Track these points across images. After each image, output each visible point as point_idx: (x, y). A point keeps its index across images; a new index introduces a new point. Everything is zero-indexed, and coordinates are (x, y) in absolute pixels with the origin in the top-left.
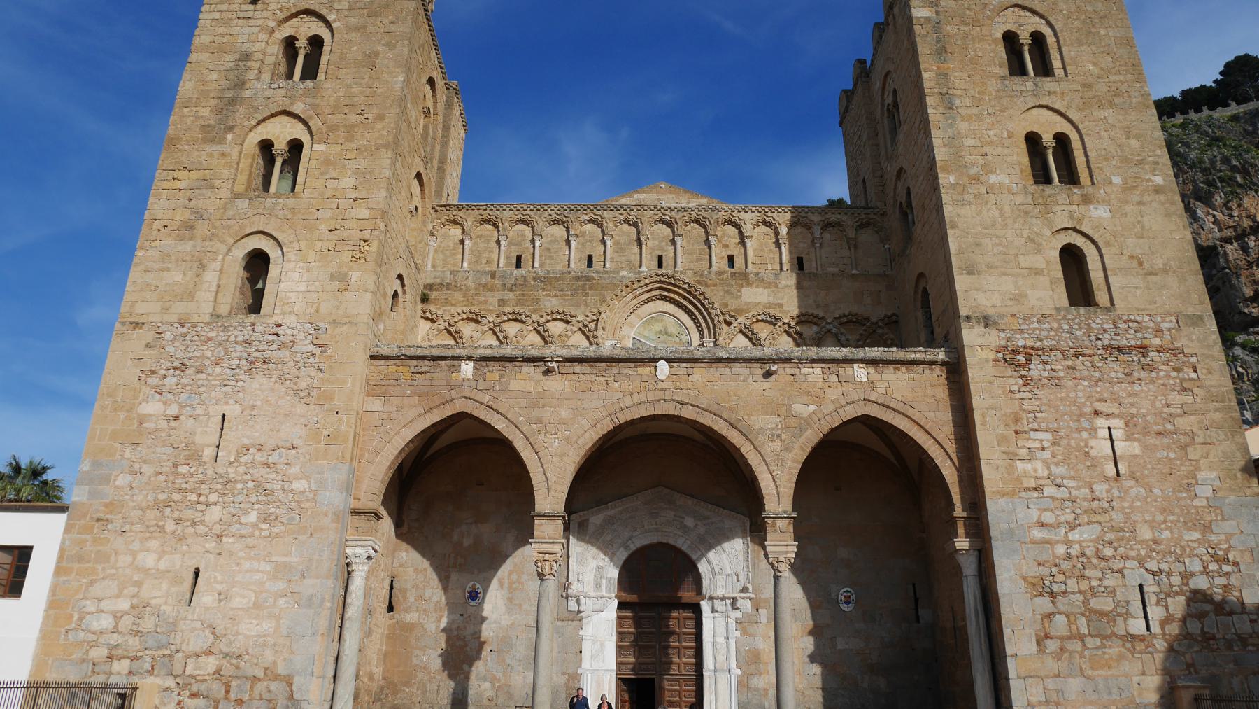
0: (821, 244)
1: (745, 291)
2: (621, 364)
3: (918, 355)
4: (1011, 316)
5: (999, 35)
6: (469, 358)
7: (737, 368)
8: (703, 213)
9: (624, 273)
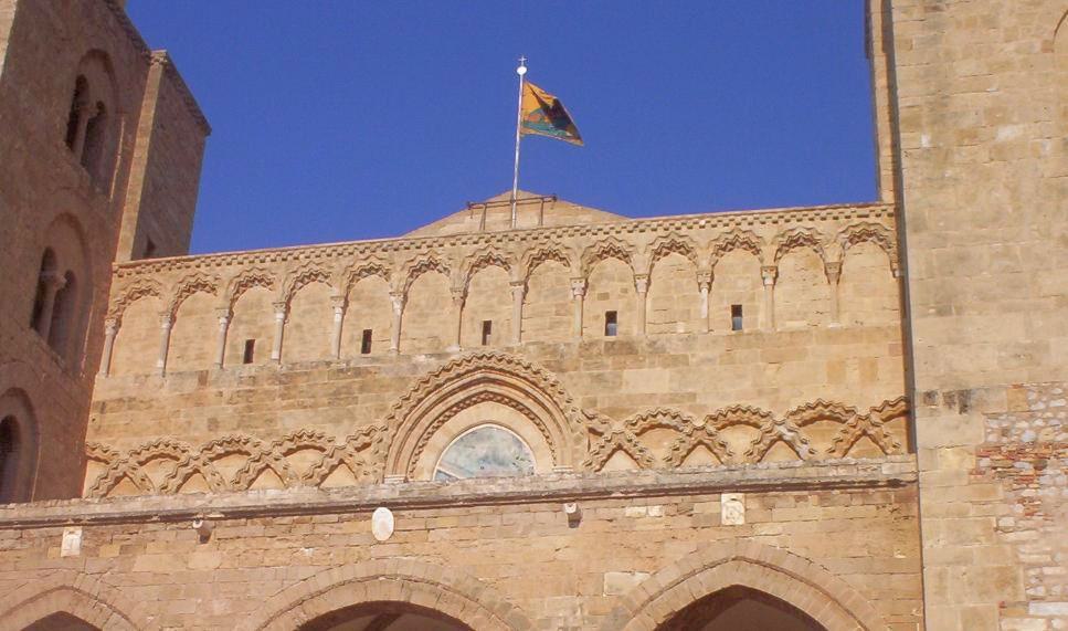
0: (775, 279)
1: (627, 374)
2: (317, 518)
3: (842, 472)
4: (1015, 387)
6: (77, 522)
7: (513, 513)
8: (566, 240)
9: (422, 359)
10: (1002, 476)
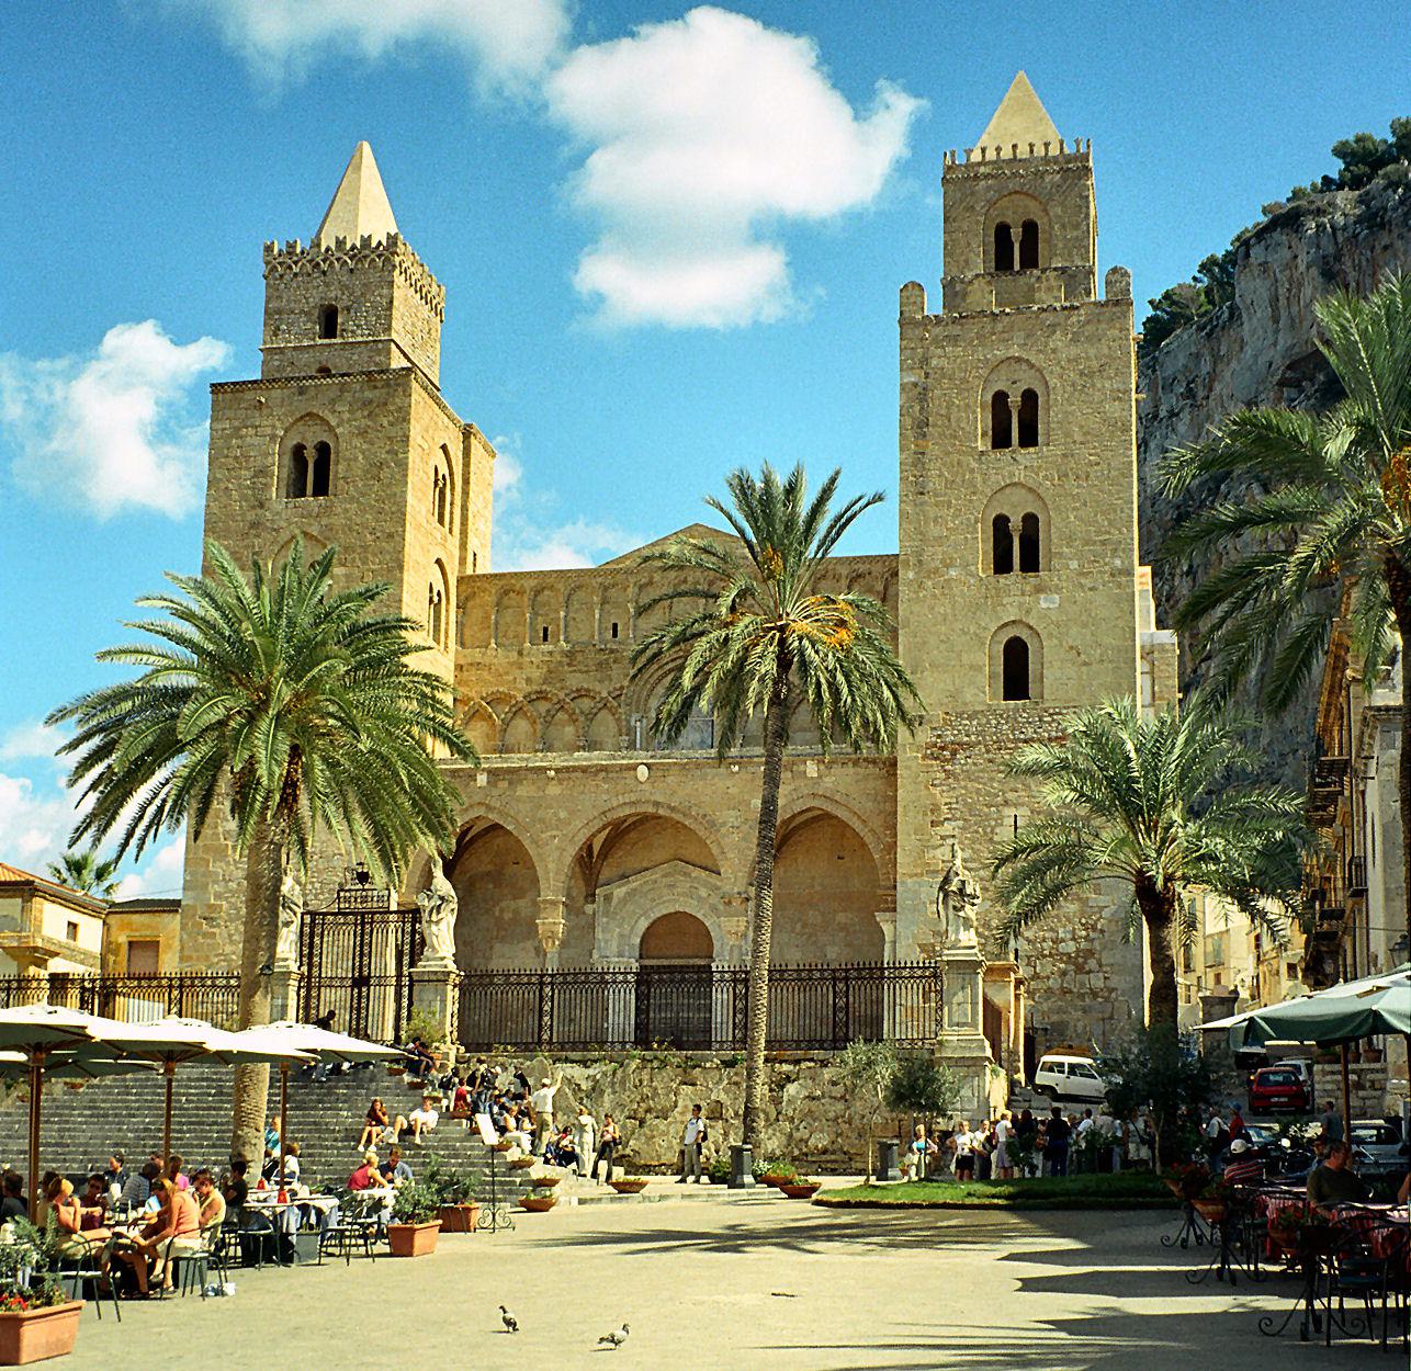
5: (989, 398)
10: (936, 759)
